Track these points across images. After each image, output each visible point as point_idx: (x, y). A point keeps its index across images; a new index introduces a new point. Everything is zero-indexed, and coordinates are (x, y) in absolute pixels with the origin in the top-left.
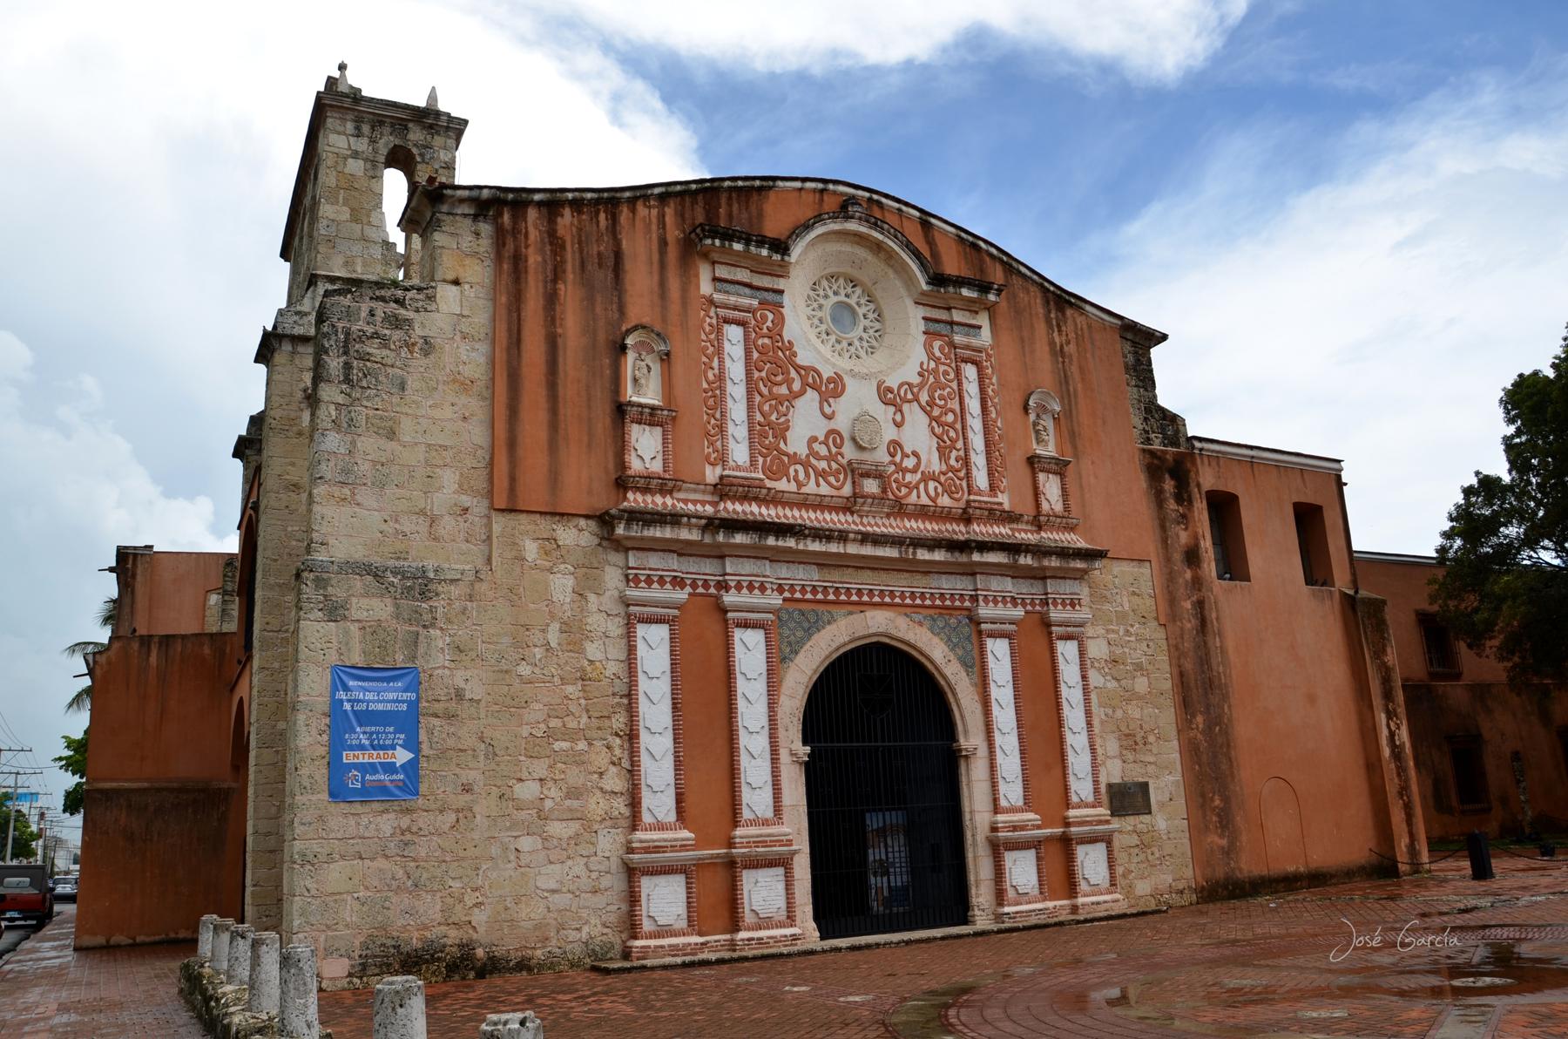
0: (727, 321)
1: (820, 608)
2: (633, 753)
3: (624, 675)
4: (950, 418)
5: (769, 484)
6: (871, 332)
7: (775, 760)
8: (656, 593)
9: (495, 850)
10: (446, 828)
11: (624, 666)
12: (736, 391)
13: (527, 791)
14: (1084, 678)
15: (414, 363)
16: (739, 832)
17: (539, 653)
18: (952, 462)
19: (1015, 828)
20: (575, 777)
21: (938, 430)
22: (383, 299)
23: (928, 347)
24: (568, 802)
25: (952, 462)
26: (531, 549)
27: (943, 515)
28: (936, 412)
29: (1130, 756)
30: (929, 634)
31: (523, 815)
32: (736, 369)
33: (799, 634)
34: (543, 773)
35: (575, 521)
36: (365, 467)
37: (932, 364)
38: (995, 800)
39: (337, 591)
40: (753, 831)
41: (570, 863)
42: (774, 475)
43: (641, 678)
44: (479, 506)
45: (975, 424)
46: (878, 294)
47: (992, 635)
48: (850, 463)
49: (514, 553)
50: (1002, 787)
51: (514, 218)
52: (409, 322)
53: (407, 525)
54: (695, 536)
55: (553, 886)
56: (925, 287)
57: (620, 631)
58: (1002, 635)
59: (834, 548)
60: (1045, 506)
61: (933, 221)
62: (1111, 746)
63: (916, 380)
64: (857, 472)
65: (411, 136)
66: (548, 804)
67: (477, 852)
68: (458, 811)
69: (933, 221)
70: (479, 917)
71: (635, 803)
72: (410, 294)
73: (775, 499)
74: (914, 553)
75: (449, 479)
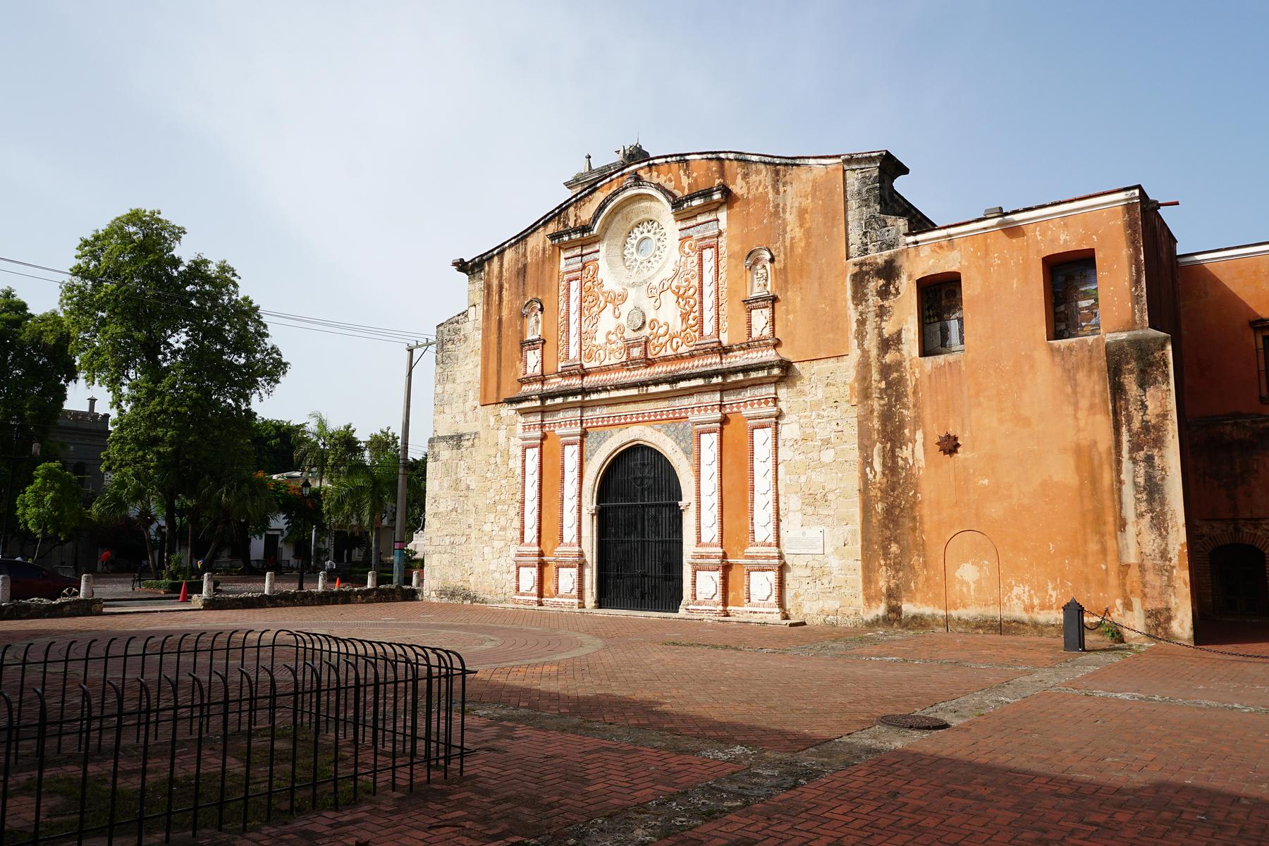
4: (692, 290)
16: (559, 549)
19: (702, 557)
20: (503, 522)
23: (681, 247)
25: (691, 322)
26: (492, 420)
29: (810, 510)
42: (590, 357)
58: (710, 432)
60: (755, 334)
61: (688, 157)
64: (629, 346)
69: (688, 157)
71: (522, 533)
73: (584, 373)
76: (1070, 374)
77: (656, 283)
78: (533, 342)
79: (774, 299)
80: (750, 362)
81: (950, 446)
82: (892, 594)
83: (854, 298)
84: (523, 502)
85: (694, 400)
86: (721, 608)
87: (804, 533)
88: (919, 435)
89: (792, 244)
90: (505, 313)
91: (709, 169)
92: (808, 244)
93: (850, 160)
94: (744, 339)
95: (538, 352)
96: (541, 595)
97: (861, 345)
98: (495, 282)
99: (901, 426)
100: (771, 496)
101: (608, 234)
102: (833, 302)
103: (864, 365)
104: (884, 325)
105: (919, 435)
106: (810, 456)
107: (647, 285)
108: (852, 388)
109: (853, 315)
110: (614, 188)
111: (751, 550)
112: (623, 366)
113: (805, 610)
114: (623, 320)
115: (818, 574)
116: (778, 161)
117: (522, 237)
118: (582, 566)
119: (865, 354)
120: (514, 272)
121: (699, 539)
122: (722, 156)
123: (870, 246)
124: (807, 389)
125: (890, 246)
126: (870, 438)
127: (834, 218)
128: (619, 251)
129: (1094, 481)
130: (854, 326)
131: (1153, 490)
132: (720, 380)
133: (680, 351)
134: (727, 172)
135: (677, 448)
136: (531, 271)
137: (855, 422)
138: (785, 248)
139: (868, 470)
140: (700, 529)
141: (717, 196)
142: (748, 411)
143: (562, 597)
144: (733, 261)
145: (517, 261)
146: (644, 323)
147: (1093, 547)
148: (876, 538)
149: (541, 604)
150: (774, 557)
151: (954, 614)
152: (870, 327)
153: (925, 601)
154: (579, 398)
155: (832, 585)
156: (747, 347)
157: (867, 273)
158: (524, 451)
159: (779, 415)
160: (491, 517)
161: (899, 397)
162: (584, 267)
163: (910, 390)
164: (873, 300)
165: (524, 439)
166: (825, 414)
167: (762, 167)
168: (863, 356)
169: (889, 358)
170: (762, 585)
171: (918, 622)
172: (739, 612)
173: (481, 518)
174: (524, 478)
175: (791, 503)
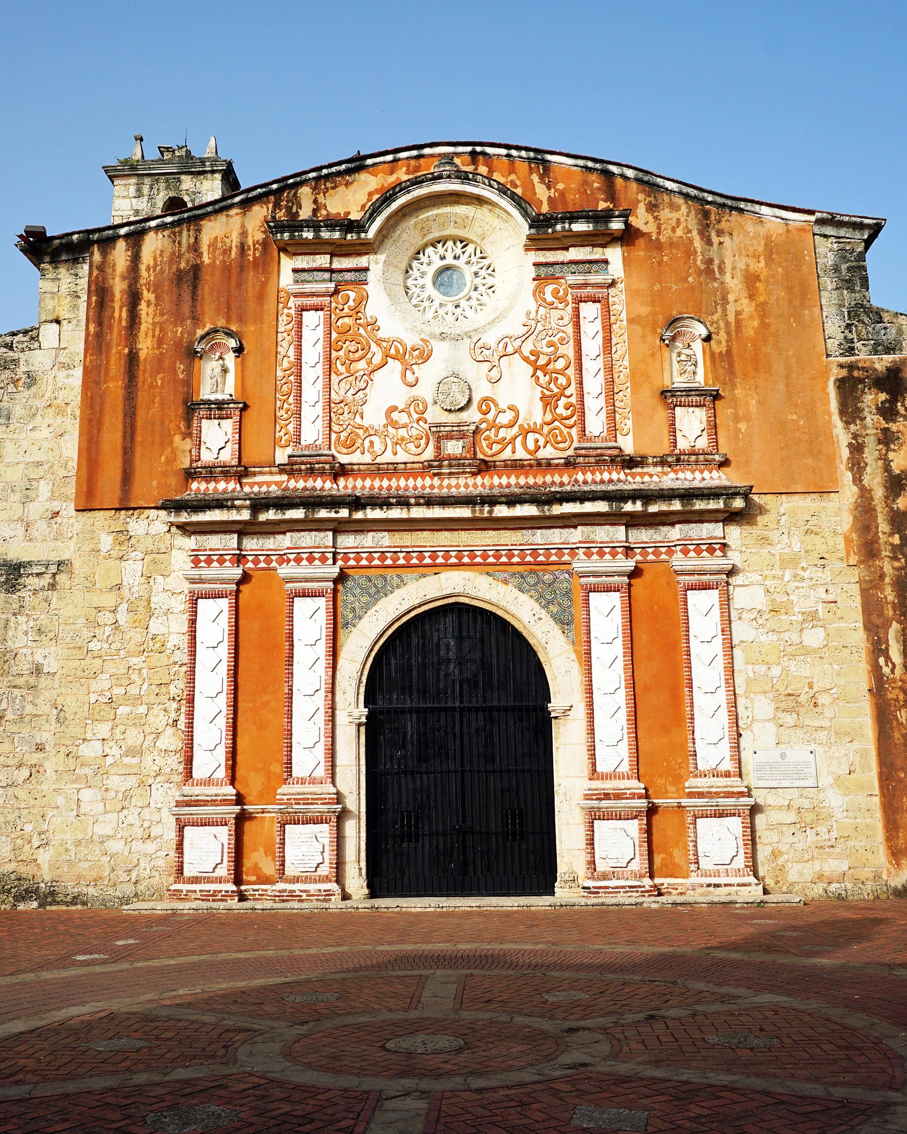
0: (304, 309)
1: (390, 573)
2: (190, 715)
4: (560, 364)
6: (482, 289)
8: (214, 571)
9: (60, 800)
10: (20, 781)
11: (186, 638)
15: (16, 396)
17: (108, 630)
19: (607, 796)
20: (134, 737)
21: (543, 380)
23: (538, 293)
24: (126, 760)
25: (561, 410)
26: (106, 542)
27: (546, 466)
28: (542, 361)
29: (790, 719)
30: (516, 592)
31: (87, 771)
32: (313, 352)
34: (107, 735)
35: (147, 512)
37: (542, 311)
38: (594, 764)
41: (125, 812)
42: (350, 446)
45: (593, 367)
46: (489, 249)
47: (595, 589)
49: (92, 546)
50: (601, 752)
51: (104, 254)
52: (16, 362)
54: (245, 515)
55: (111, 833)
58: (608, 589)
59: (396, 513)
61: (549, 157)
64: (440, 435)
65: (184, 186)
66: (109, 760)
67: (44, 801)
69: (549, 157)
70: (44, 857)
72: (17, 339)
73: (340, 471)
74: (491, 512)
75: (44, 488)
77: (490, 338)
78: (220, 405)
79: (716, 397)
80: (697, 484)
83: (842, 412)
84: (191, 701)
85: (576, 535)
86: (647, 882)
87: (783, 756)
89: (738, 322)
90: (145, 346)
91: (585, 183)
92: (764, 326)
93: (831, 221)
94: (665, 448)
95: (228, 425)
96: (238, 881)
97: (858, 480)
98: (119, 287)
100: (722, 697)
101: (388, 243)
102: (810, 413)
103: (865, 510)
104: (891, 455)
106: (786, 636)
107: (458, 338)
108: (848, 540)
109: (842, 436)
110: (402, 175)
111: (693, 783)
112: (429, 468)
113: (792, 876)
114: (425, 391)
115: (809, 818)
116: (710, 198)
118: (342, 816)
119: (865, 493)
122: (614, 169)
123: (858, 345)
124: (774, 536)
125: (889, 350)
126: (881, 615)
127: (803, 296)
128: (401, 278)
130: (845, 453)
132: (638, 506)
133: (541, 454)
135: (543, 613)
136: (209, 283)
137: (856, 589)
138: (727, 324)
139: (882, 661)
141: (617, 225)
142: (678, 561)
143: (296, 880)
144: (637, 329)
145: (176, 257)
146: (470, 401)
149: (242, 898)
150: (741, 794)
152: (871, 454)
154: (344, 513)
155: (834, 834)
156: (674, 460)
157: (861, 381)
158: (194, 603)
159: (732, 572)
160: (103, 729)
162: (336, 292)
164: (872, 420)
165: (193, 581)
166: (806, 575)
167: (680, 201)
168: (861, 496)
172: (687, 888)
173: (74, 730)
174: (193, 653)
175: (758, 708)
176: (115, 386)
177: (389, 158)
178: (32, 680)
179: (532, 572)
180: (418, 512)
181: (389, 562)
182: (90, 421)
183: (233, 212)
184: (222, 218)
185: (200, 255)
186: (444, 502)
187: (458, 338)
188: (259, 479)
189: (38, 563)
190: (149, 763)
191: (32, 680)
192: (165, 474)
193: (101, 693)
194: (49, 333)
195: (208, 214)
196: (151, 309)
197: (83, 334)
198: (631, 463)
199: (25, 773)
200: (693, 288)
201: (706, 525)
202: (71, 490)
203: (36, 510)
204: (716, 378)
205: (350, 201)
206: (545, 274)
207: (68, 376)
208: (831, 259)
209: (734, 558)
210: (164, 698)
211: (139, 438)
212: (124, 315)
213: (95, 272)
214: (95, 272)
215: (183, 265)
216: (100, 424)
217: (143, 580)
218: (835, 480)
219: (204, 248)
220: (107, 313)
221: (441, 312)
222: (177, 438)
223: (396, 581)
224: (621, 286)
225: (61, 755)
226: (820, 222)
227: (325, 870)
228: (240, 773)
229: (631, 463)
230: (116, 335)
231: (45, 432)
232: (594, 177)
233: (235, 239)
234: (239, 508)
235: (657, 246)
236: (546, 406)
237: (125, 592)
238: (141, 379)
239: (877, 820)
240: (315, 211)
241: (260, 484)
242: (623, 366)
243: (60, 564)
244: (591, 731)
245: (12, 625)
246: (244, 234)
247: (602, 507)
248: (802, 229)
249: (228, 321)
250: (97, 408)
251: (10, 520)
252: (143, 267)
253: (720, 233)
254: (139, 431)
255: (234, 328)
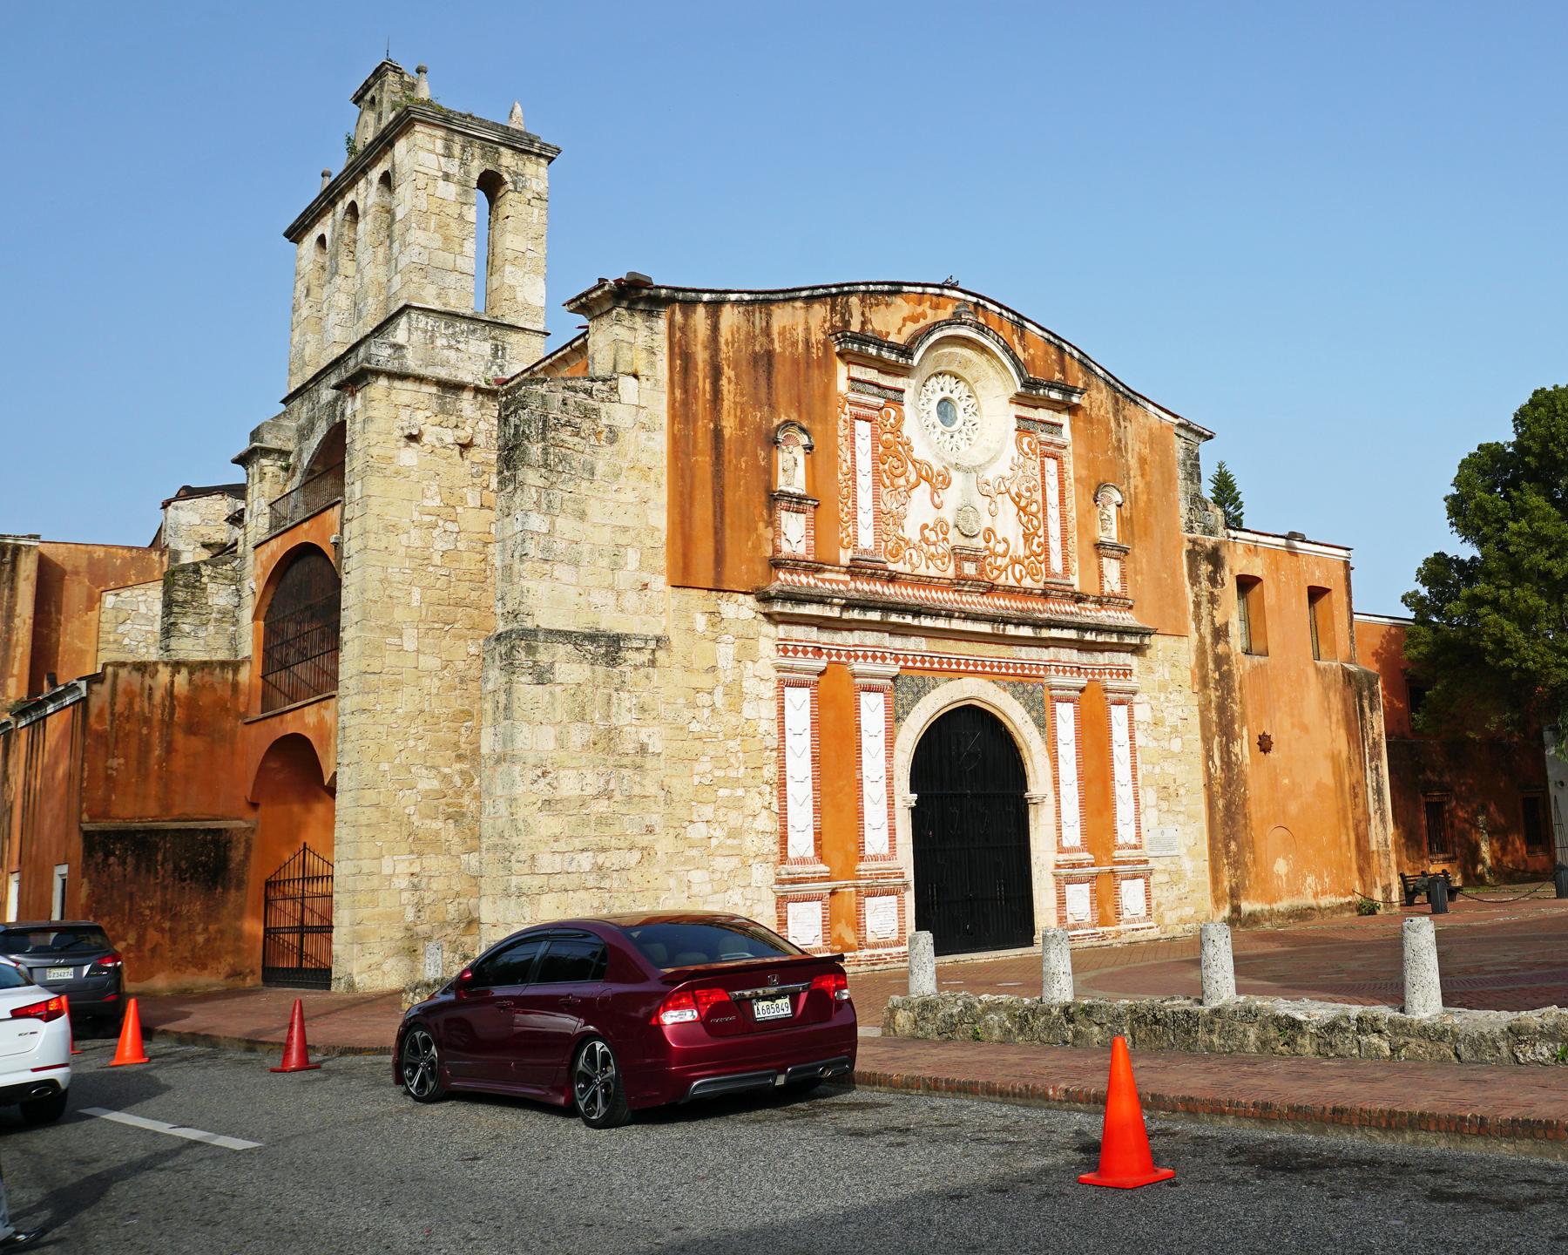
1: (928, 675)
2: (783, 797)
3: (775, 730)
4: (1034, 508)
5: (891, 567)
7: (891, 805)
8: (801, 662)
9: (672, 882)
10: (633, 863)
12: (865, 482)
13: (697, 831)
14: (1131, 738)
17: (707, 712)
18: (1034, 547)
19: (1074, 866)
20: (734, 819)
21: (1025, 519)
22: (574, 389)
23: (1019, 442)
24: (729, 842)
25: (1034, 547)
26: (701, 622)
27: (1028, 593)
28: (1023, 504)
29: (1164, 805)
31: (694, 852)
32: (864, 463)
33: (910, 697)
34: (710, 816)
36: (560, 546)
39: (543, 657)
40: (874, 865)
43: (788, 734)
44: (660, 583)
45: (1053, 513)
46: (979, 392)
48: (953, 549)
50: (1065, 831)
51: (686, 316)
52: (596, 411)
53: (596, 598)
56: (1020, 389)
57: (772, 694)
59: (941, 623)
60: (1107, 589)
61: (1028, 325)
62: (1149, 797)
63: (1008, 474)
64: (959, 555)
66: (714, 842)
68: (643, 849)
69: (1028, 325)
71: (784, 840)
73: (893, 578)
76: (1326, 689)
78: (800, 499)
81: (1265, 744)
82: (1234, 894)
83: (1190, 576)
84: (783, 784)
86: (1099, 930)
88: (1245, 733)
90: (729, 425)
91: (1046, 353)
92: (1150, 501)
93: (1186, 427)
97: (1198, 629)
98: (701, 356)
99: (1232, 722)
102: (1174, 574)
103: (1201, 651)
105: (1245, 733)
108: (1193, 673)
114: (948, 515)
117: (764, 301)
119: (1202, 638)
120: (746, 353)
121: (1059, 842)
125: (1212, 533)
129: (1342, 784)
131: (1379, 791)
134: (1068, 370)
136: (782, 372)
140: (1054, 830)
143: (876, 946)
145: (751, 338)
147: (1344, 839)
148: (1220, 837)
151: (1275, 906)
152: (1204, 611)
153: (1257, 898)
154: (909, 619)
160: (707, 811)
161: (1230, 690)
163: (1237, 685)
164: (1205, 584)
165: (779, 669)
167: (1102, 385)
169: (1221, 648)
170: (1131, 894)
171: (1254, 919)
174: (783, 738)
175: (1149, 797)
176: (704, 461)
177: (919, 289)
178: (638, 760)
179: (1021, 682)
180: (957, 625)
181: (927, 665)
182: (682, 494)
183: (799, 304)
184: (788, 307)
185: (772, 341)
186: (976, 618)
187: (956, 469)
188: (827, 576)
189: (636, 637)
190: (751, 843)
191: (638, 760)
192: (751, 560)
193: (703, 775)
194: (627, 385)
195: (778, 301)
196: (732, 387)
197: (665, 398)
198: (1079, 599)
199: (636, 855)
200: (1110, 461)
201: (1122, 655)
202: (662, 562)
203: (624, 578)
204: (1124, 538)
205: (892, 321)
206: (1025, 426)
207: (649, 439)
208: (1180, 455)
209: (1133, 682)
210: (758, 781)
211: (728, 520)
212: (708, 387)
213: (678, 335)
214: (678, 335)
215: (757, 348)
216: (691, 497)
217: (735, 664)
218: (1186, 627)
219: (775, 336)
220: (692, 381)
221: (942, 439)
222: (761, 525)
223: (932, 682)
224: (1070, 449)
225: (671, 837)
226: (1180, 425)
227: (895, 937)
228: (826, 851)
229: (1079, 599)
230: (701, 406)
231: (629, 496)
232: (1052, 349)
233: (800, 334)
234: (831, 605)
235: (1090, 420)
236: (1026, 541)
237: (721, 674)
238: (726, 458)
239: (1206, 878)
240: (863, 323)
241: (830, 581)
242: (1073, 515)
243: (658, 640)
244: (1058, 814)
245: (614, 700)
246: (807, 329)
247: (1071, 634)
248: (1168, 428)
249: (800, 416)
250: (688, 480)
251: (600, 587)
252: (722, 340)
253: (1125, 418)
254: (727, 512)
255: (805, 424)
